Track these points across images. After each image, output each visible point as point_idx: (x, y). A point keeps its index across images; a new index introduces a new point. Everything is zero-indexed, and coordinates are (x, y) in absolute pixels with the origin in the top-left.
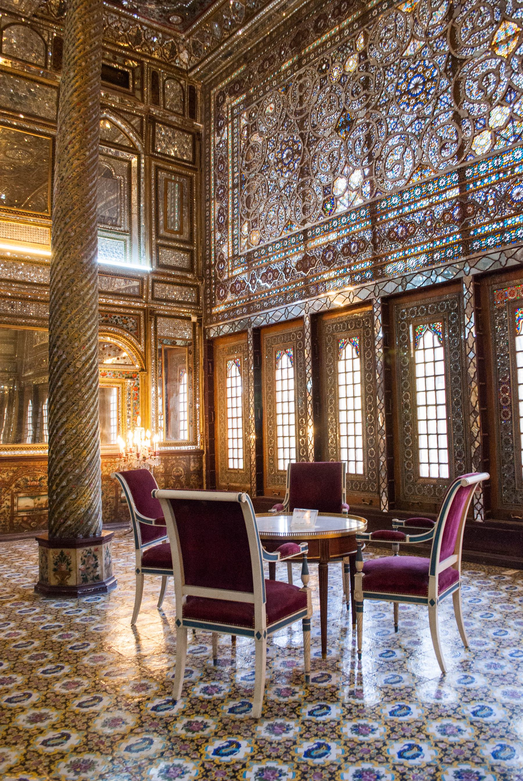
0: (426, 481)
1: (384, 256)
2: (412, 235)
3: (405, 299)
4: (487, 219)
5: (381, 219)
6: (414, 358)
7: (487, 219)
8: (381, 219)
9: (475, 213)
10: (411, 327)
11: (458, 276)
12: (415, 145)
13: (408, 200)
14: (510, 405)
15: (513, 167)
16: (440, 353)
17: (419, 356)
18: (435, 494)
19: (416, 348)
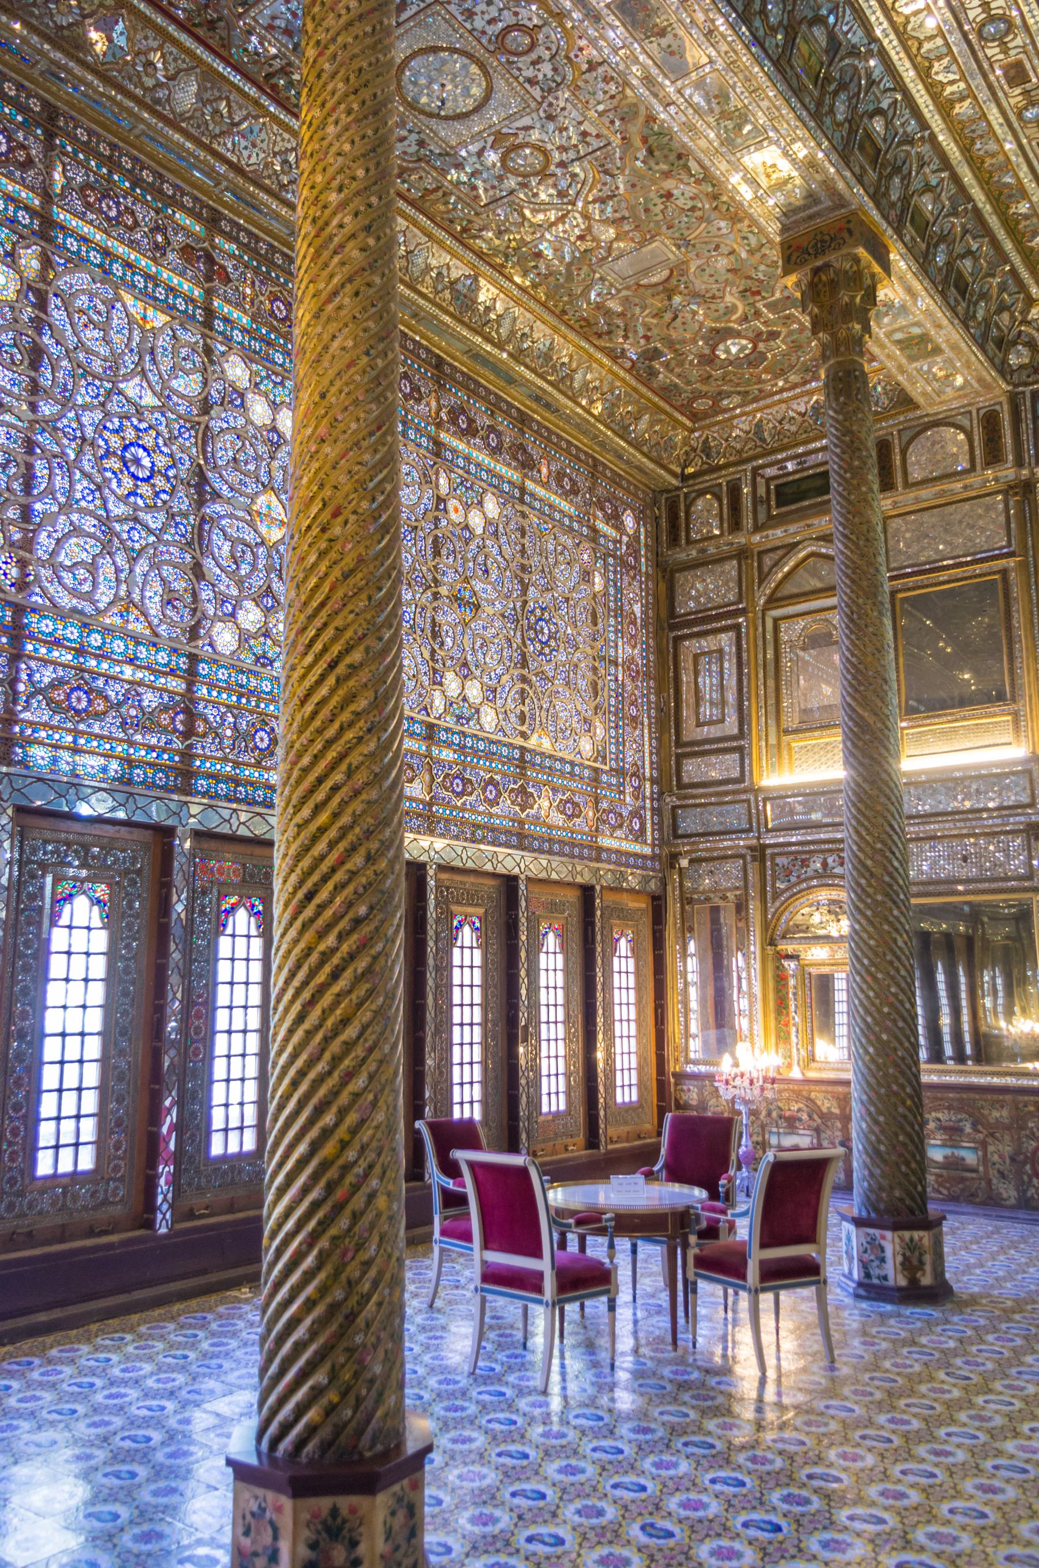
0: (48, 1184)
1: (31, 723)
2: (99, 716)
3: (45, 822)
4: (220, 754)
5: (36, 650)
6: (48, 940)
7: (220, 754)
8: (36, 650)
9: (204, 735)
10: (49, 879)
11: (169, 822)
12: (121, 559)
13: (100, 648)
14: (204, 1038)
15: (259, 699)
16: (100, 940)
17: (59, 939)
18: (64, 1205)
19: (53, 923)
